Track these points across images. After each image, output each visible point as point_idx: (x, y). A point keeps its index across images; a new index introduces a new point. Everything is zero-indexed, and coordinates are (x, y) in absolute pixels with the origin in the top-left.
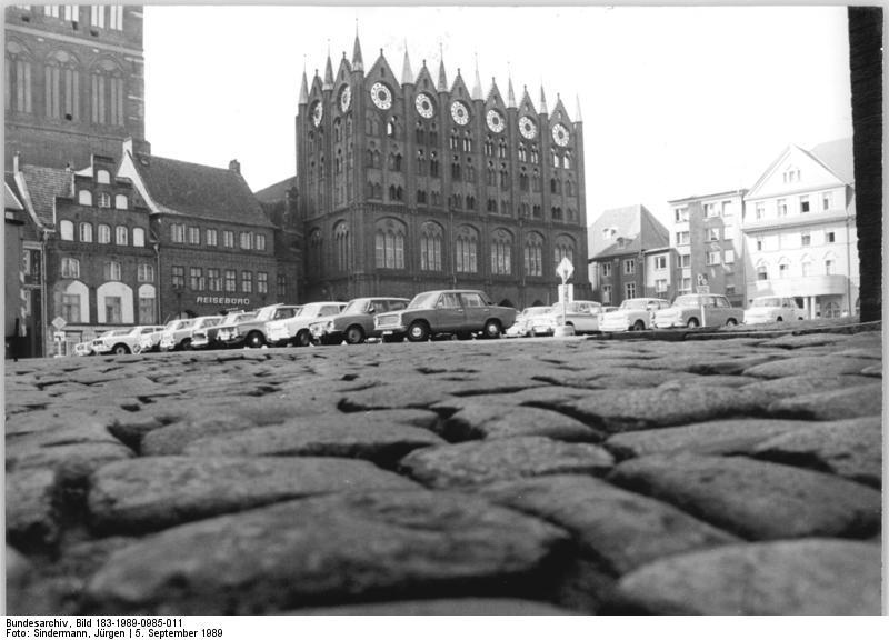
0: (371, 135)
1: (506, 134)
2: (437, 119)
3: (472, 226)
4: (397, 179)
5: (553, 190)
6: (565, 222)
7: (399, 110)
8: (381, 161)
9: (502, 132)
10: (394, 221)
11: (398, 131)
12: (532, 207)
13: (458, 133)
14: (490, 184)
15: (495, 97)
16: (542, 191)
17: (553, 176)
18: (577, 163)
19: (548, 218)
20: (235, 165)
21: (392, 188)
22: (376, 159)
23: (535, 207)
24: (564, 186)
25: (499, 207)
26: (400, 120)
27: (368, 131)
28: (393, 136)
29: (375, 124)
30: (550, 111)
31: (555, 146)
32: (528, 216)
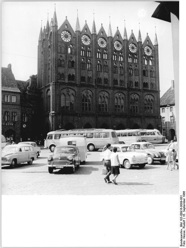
0: (61, 53)
1: (122, 51)
3: (106, 91)
4: (72, 72)
6: (149, 89)
9: (121, 50)
10: (70, 89)
12: (134, 82)
13: (101, 51)
14: (115, 73)
15: (118, 35)
17: (144, 69)
18: (156, 63)
19: (141, 87)
20: (10, 65)
22: (63, 63)
24: (149, 73)
25: (119, 82)
26: (74, 46)
27: (59, 51)
29: (63, 48)
30: (143, 40)
31: (145, 55)
32: (133, 86)
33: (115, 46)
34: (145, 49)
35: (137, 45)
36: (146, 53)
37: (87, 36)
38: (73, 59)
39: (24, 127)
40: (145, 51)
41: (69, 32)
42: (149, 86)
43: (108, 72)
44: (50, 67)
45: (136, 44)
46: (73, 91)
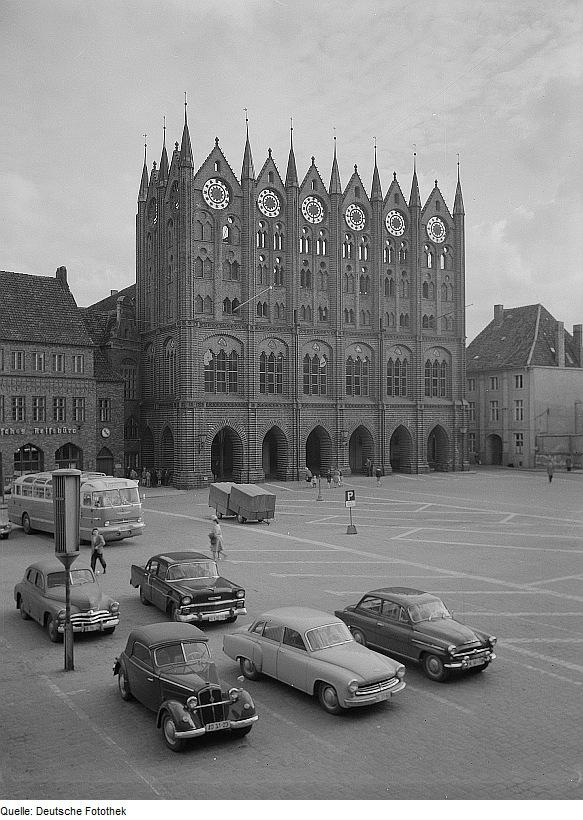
2: (283, 219)
4: (232, 291)
5: (426, 296)
6: (439, 333)
7: (236, 210)
8: (212, 271)
11: (235, 233)
16: (411, 296)
17: (425, 279)
20: (62, 272)
21: (226, 301)
23: (402, 316)
26: (237, 221)
27: (197, 236)
28: (228, 240)
29: (207, 228)
31: (429, 243)
33: (348, 219)
34: (429, 226)
35: (408, 215)
36: (431, 237)
37: (272, 194)
38: (235, 258)
39: (104, 435)
40: (429, 232)
41: (224, 182)
42: (439, 324)
43: (328, 290)
44: (173, 279)
45: (406, 211)
46: (235, 342)
